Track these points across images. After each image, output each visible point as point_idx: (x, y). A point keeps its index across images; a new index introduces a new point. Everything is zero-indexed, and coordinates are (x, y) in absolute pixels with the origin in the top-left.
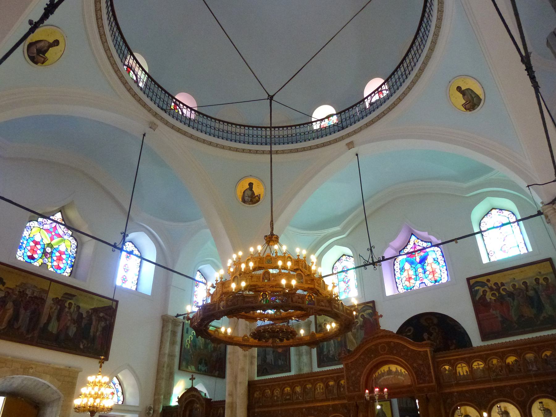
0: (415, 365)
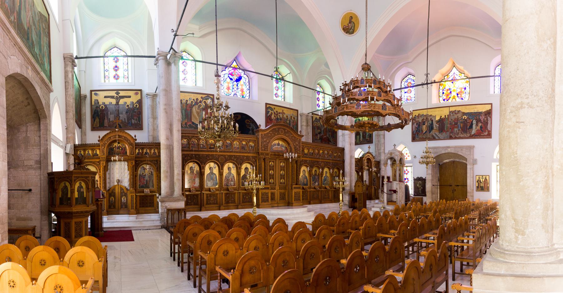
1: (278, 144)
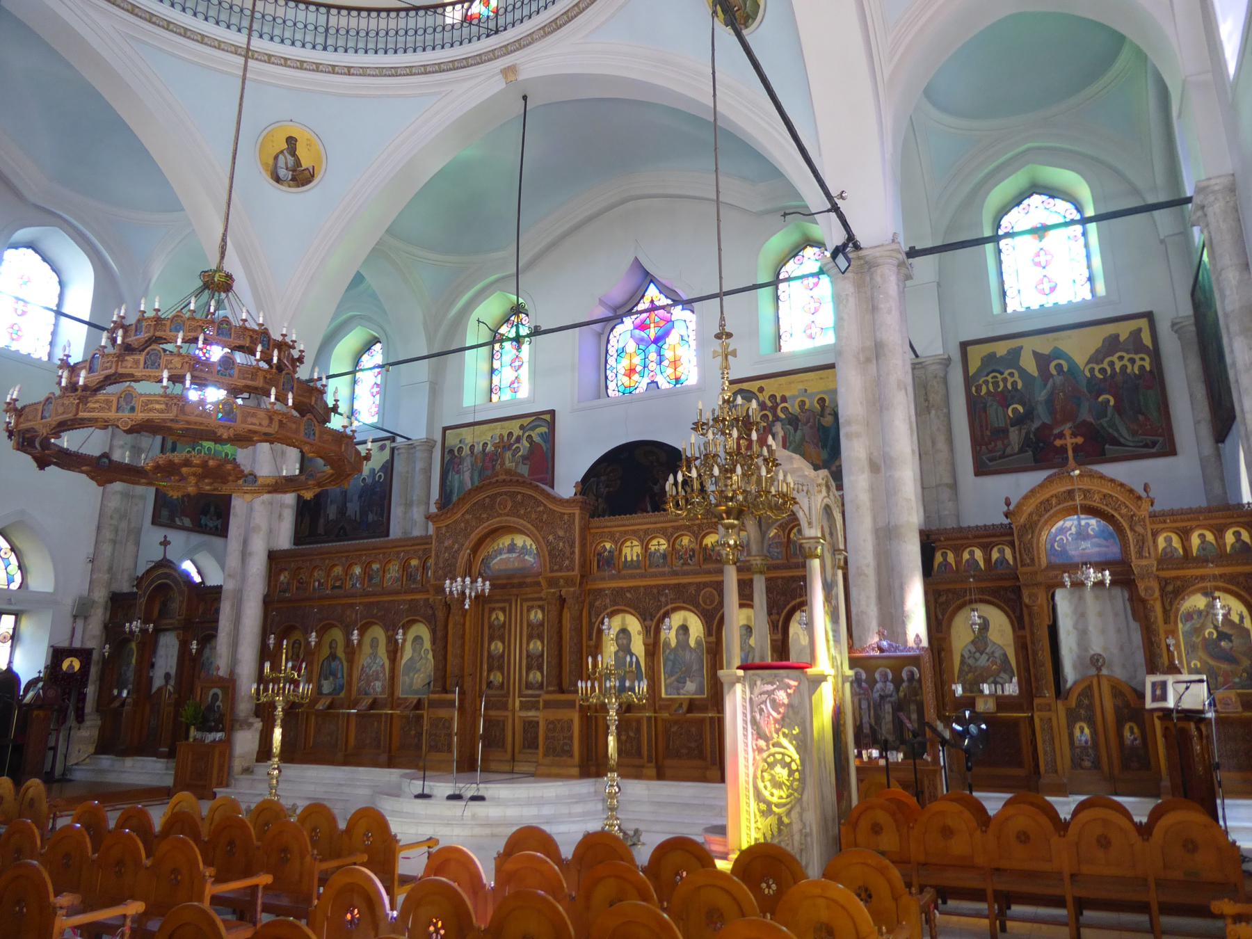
0: (551, 538)
1: (512, 548)
